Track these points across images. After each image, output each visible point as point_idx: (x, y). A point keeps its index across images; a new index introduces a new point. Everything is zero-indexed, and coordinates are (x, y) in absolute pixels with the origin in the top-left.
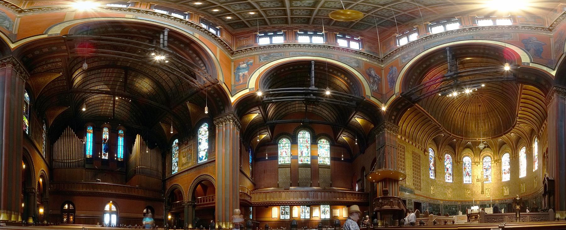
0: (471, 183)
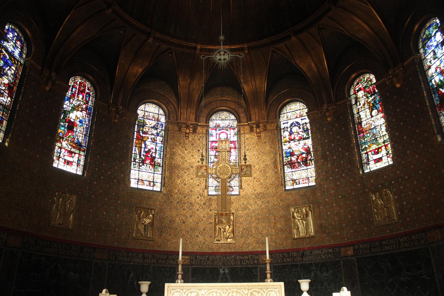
0: (157, 188)
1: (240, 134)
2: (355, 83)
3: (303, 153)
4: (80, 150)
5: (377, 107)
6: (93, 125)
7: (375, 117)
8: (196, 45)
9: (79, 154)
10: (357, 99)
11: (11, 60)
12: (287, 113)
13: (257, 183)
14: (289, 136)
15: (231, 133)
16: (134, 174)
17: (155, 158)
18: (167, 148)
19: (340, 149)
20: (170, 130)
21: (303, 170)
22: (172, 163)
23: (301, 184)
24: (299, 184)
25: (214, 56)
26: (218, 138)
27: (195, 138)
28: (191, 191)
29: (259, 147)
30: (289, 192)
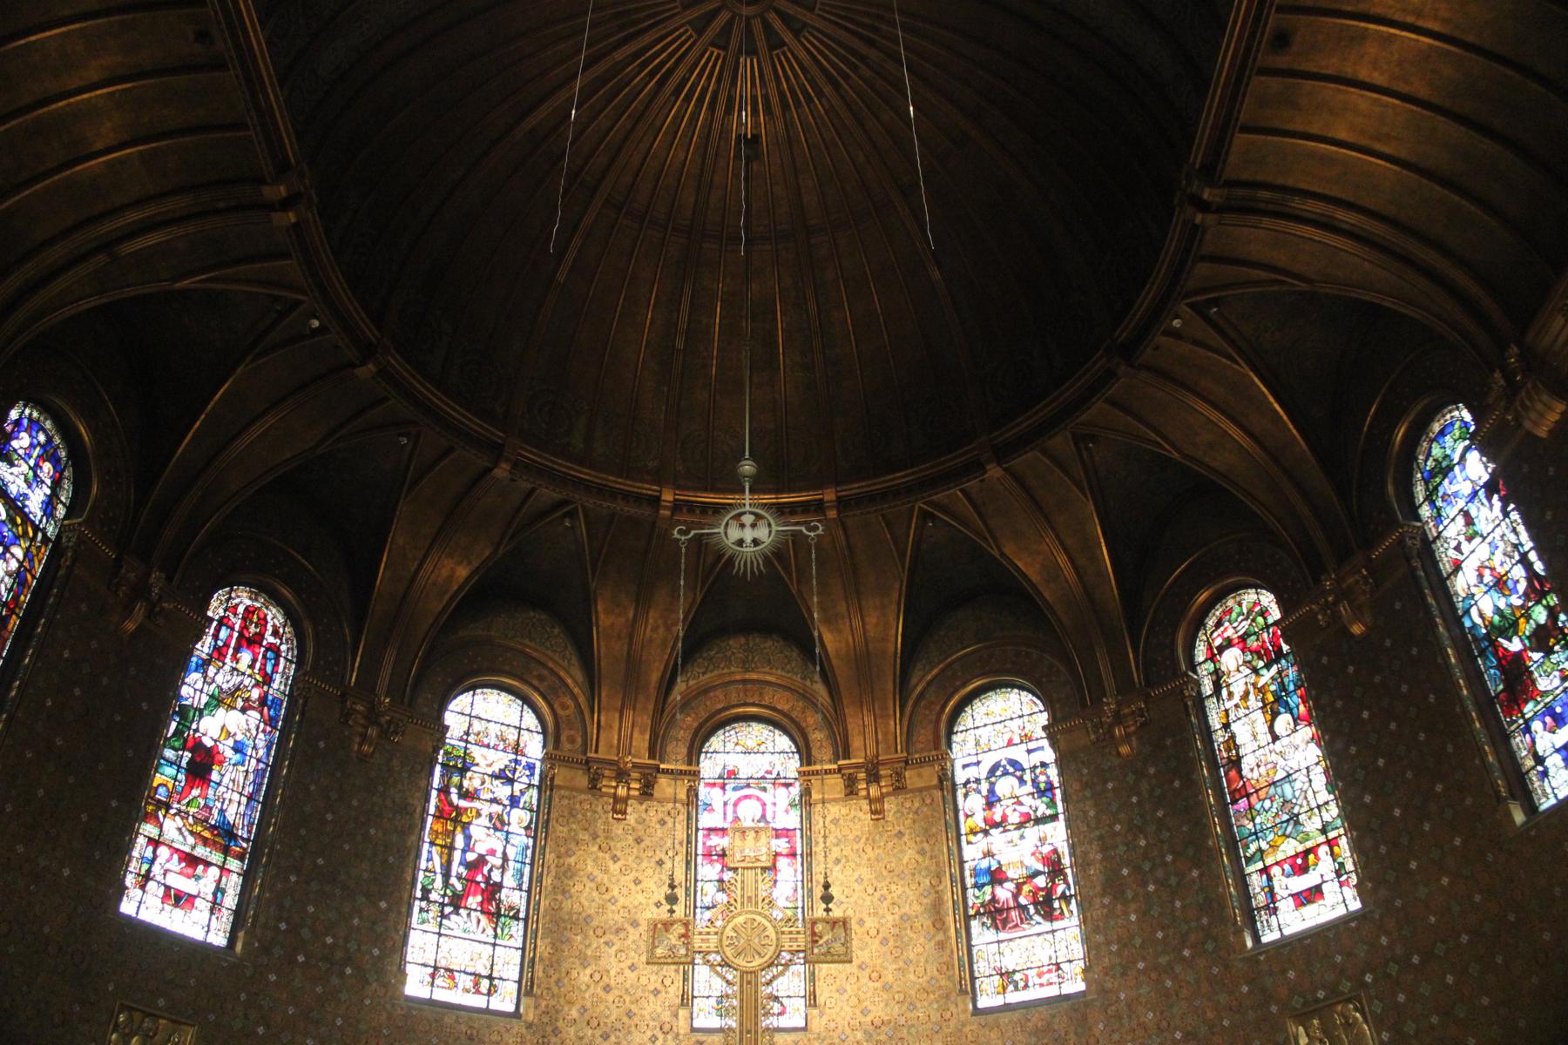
0: (504, 1001)
1: (810, 805)
2: (1211, 622)
3: (1037, 873)
4: (226, 851)
5: (1292, 705)
6: (283, 761)
7: (1285, 741)
8: (660, 492)
9: (223, 869)
10: (1217, 675)
11: (14, 524)
12: (977, 728)
13: (871, 984)
14: (984, 810)
15: (776, 801)
17: (499, 886)
18: (548, 850)
19: (1169, 858)
20: (560, 787)
21: (1039, 934)
22: (560, 908)
23: (1031, 989)
24: (1026, 986)
25: (721, 530)
26: (730, 817)
27: (648, 819)
28: (630, 1014)
29: (877, 851)
30: (990, 1018)
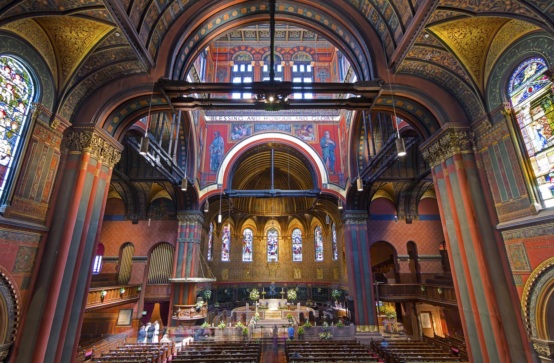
0: (251, 261)
16: (243, 256)
